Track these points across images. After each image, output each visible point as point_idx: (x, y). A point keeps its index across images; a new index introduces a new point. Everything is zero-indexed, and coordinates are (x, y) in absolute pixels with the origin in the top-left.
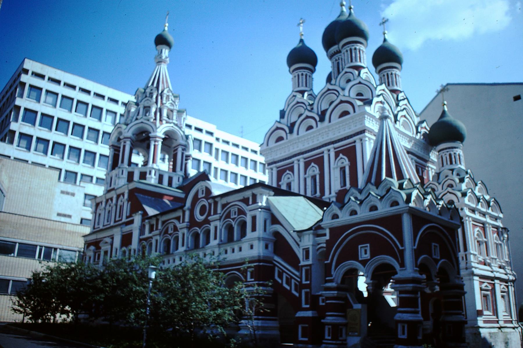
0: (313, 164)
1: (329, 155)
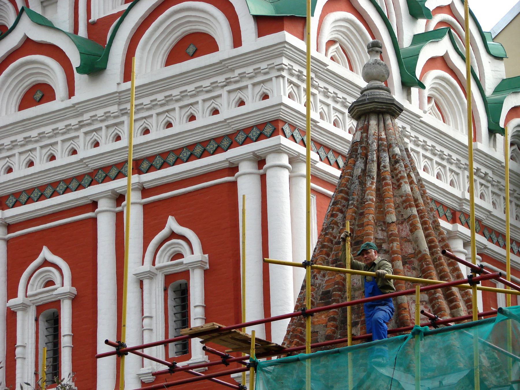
0: (46, 253)
1: (119, 218)
